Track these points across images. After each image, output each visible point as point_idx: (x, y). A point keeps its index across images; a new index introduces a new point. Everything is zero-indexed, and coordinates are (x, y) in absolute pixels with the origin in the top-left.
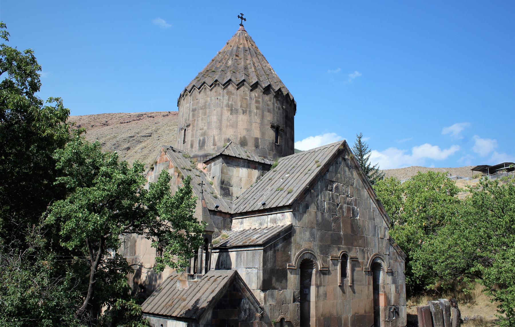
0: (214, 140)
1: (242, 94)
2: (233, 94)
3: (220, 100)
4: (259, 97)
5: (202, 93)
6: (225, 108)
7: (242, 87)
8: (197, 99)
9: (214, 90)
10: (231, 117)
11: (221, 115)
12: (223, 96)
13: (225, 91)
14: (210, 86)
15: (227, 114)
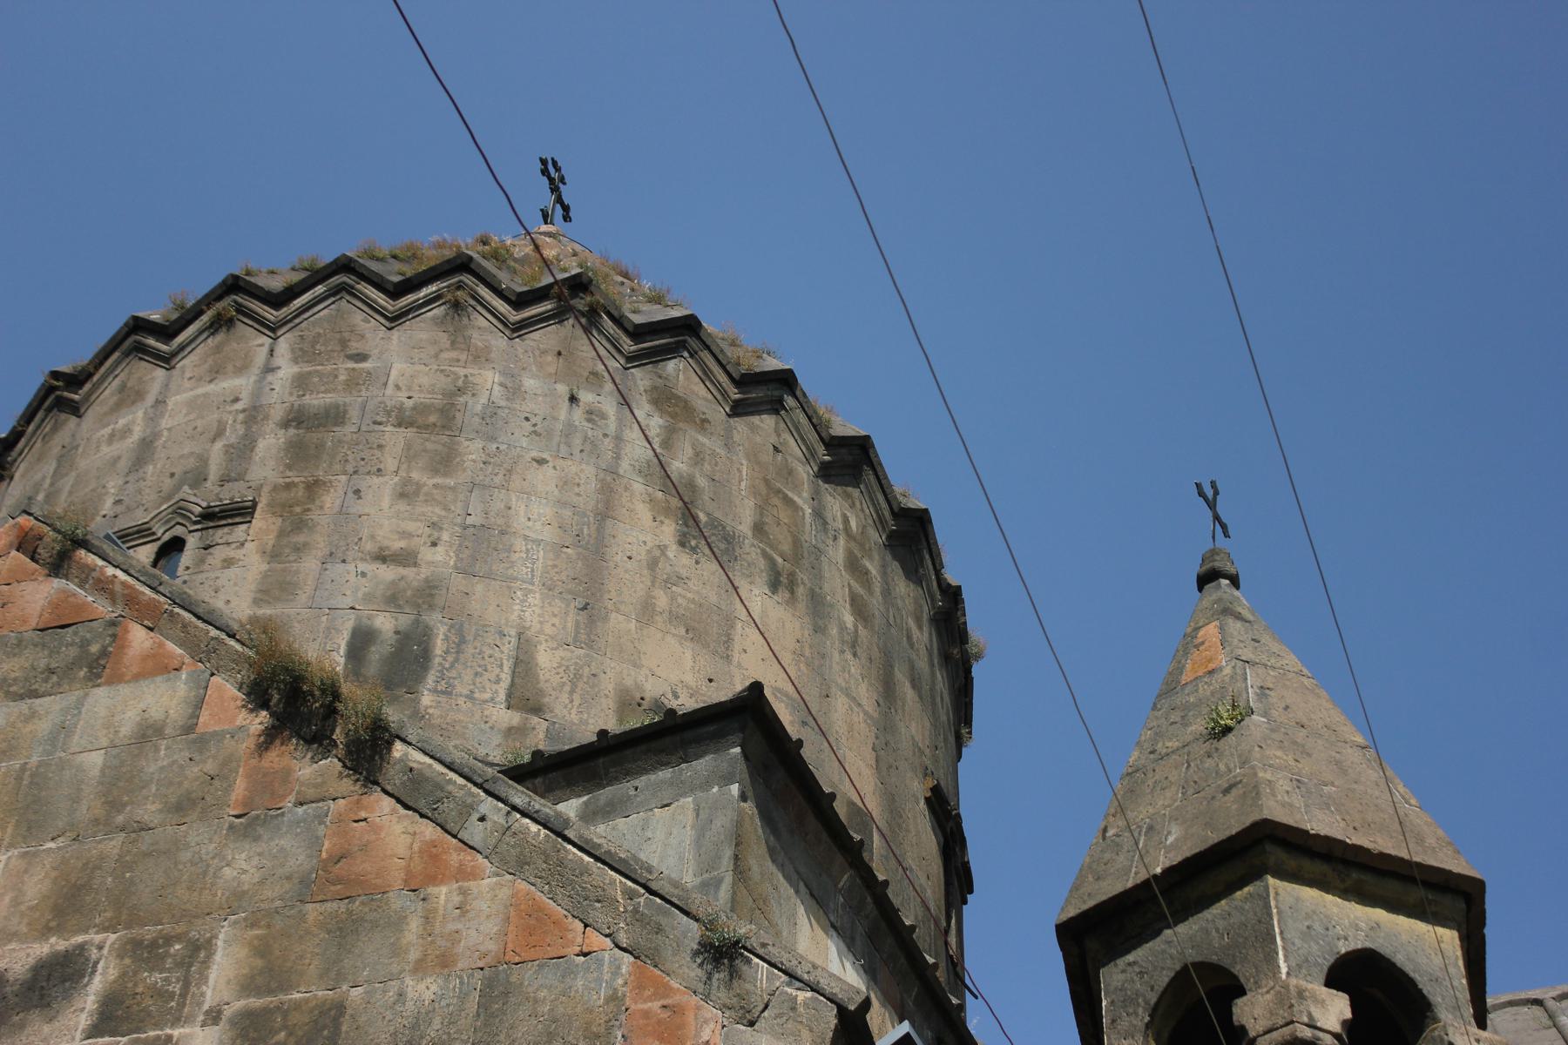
0: (523, 664)
1: (767, 456)
2: (704, 424)
3: (592, 415)
4: (868, 553)
5: (424, 330)
6: (638, 487)
7: (767, 422)
8: (361, 357)
9: (546, 338)
10: (682, 561)
11: (605, 512)
12: (625, 402)
13: (641, 378)
14: (519, 301)
15: (643, 530)
